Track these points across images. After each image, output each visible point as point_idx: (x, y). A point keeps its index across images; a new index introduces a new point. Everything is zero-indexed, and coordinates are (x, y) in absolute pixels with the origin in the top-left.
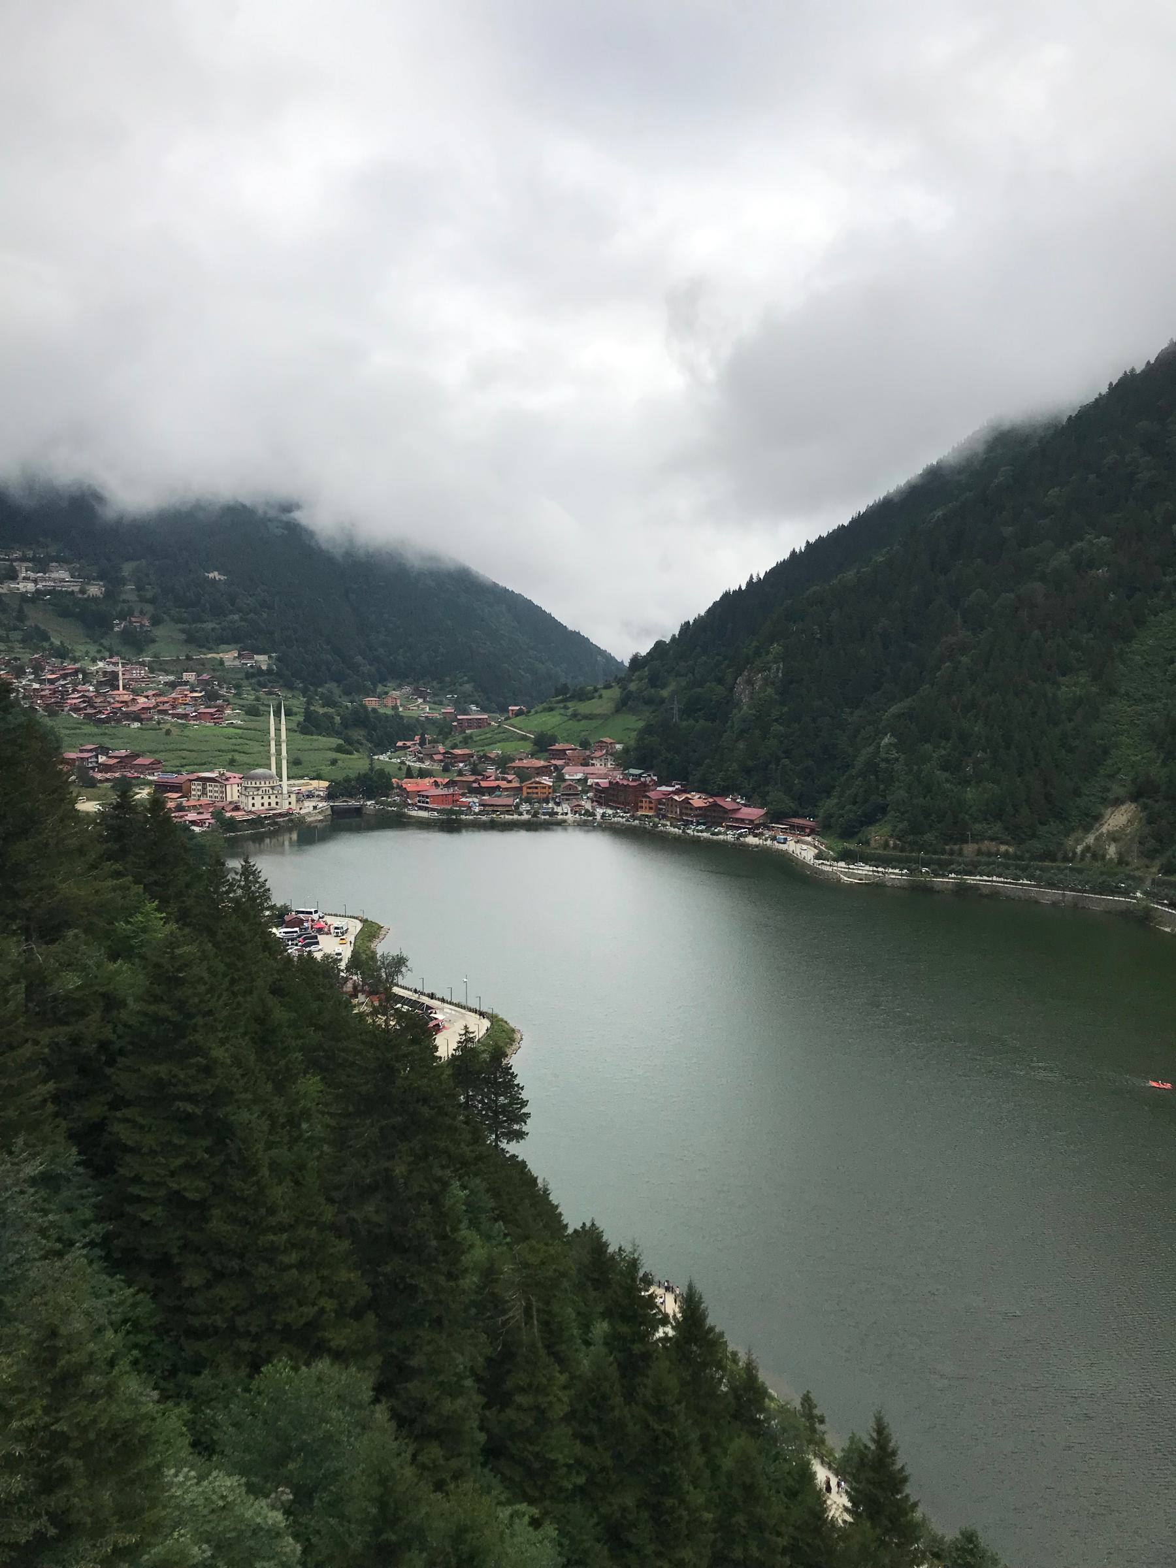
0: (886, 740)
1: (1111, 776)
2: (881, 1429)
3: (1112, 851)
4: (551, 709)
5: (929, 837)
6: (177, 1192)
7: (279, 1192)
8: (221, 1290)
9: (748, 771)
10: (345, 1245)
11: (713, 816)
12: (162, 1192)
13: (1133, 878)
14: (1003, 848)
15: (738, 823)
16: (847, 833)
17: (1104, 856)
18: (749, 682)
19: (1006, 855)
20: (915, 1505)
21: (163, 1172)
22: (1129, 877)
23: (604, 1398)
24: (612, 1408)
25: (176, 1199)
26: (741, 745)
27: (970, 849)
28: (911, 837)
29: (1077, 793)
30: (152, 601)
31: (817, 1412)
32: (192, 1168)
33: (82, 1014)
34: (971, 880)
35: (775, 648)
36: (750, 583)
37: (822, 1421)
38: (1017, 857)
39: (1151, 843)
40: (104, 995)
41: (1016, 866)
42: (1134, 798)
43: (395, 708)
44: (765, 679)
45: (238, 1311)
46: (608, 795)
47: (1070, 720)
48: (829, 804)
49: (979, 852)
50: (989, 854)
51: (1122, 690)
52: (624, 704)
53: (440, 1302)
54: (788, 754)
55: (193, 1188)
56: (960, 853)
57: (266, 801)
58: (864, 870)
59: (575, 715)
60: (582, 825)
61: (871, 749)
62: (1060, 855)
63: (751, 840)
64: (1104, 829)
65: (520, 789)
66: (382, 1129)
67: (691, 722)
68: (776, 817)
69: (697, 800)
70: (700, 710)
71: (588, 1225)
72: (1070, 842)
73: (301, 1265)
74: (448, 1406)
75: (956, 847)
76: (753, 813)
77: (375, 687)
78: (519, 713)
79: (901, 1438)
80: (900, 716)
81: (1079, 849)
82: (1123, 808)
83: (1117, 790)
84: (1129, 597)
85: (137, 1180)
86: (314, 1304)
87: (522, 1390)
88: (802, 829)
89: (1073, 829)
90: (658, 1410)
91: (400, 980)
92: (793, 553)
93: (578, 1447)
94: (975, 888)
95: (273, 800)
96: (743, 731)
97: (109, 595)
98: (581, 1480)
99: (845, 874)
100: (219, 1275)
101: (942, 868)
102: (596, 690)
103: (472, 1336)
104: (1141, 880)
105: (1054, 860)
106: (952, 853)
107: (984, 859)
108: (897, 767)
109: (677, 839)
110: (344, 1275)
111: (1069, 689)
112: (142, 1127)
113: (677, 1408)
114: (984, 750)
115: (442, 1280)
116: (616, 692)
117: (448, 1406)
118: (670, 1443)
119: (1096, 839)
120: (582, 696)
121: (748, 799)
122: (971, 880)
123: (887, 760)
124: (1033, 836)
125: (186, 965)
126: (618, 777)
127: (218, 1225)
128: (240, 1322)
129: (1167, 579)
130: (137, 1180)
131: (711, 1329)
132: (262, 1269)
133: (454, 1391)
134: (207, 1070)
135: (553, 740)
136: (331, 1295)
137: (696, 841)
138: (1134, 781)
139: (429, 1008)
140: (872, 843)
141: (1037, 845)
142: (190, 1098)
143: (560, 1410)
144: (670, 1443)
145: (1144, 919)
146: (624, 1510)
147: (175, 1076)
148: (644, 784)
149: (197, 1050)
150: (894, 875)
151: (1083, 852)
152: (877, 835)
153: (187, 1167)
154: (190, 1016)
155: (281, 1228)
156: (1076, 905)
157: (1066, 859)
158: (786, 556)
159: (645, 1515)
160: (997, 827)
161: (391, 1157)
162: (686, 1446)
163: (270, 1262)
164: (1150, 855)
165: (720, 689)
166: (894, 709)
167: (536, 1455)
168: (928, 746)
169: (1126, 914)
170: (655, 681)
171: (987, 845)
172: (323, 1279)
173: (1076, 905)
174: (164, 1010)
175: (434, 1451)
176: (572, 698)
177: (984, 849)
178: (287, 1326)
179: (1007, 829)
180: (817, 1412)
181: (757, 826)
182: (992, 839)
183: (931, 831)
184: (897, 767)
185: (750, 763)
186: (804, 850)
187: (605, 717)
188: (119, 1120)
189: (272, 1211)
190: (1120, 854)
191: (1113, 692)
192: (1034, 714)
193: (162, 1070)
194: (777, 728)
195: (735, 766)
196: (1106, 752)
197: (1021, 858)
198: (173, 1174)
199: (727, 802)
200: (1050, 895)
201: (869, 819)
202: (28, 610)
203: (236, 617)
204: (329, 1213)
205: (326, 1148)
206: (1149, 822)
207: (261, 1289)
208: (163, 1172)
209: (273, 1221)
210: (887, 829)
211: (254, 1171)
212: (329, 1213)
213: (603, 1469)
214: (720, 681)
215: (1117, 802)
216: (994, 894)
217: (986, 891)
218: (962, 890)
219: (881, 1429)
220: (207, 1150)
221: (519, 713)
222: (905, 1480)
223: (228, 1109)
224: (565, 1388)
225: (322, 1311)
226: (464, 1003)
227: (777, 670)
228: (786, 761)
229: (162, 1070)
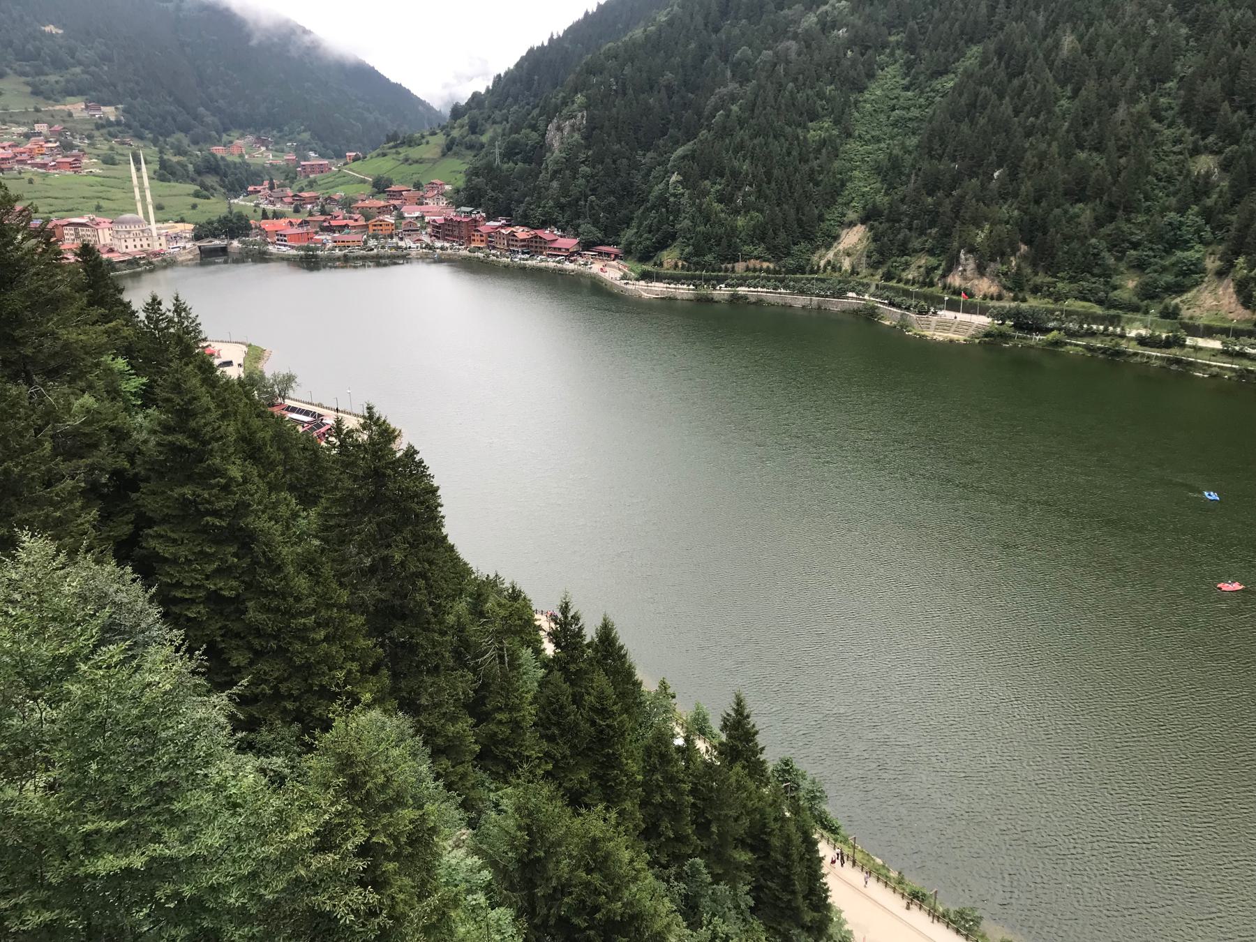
0: (674, 178)
1: (847, 204)
2: (739, 703)
3: (846, 264)
4: (384, 155)
5: (709, 258)
6: (215, 591)
7: (302, 583)
8: (263, 666)
9: (562, 208)
10: (361, 619)
11: (534, 247)
12: (202, 594)
13: (863, 285)
14: (765, 265)
15: (556, 252)
16: (645, 257)
17: (840, 268)
18: (559, 129)
19: (768, 270)
20: (763, 749)
21: (199, 577)
22: (860, 284)
23: (562, 707)
24: (568, 714)
25: (215, 598)
26: (555, 184)
27: (740, 266)
28: (695, 259)
29: (821, 218)
31: (670, 691)
32: (223, 572)
33: (95, 446)
34: (742, 290)
35: (580, 98)
36: (551, 40)
37: (674, 697)
38: (776, 272)
39: (875, 257)
40: (112, 430)
41: (777, 279)
42: (863, 223)
43: (241, 156)
44: (572, 126)
45: (280, 680)
46: (444, 230)
47: (817, 158)
48: (629, 234)
49: (748, 269)
50: (755, 270)
51: (857, 133)
52: (449, 148)
53: (436, 654)
54: (594, 190)
55: (228, 587)
56: (733, 270)
57: (138, 243)
58: (659, 288)
59: (406, 160)
60: (422, 258)
61: (661, 186)
62: (808, 268)
63: (569, 266)
64: (841, 247)
65: (367, 226)
66: (378, 525)
67: (511, 164)
68: (587, 245)
69: (521, 233)
70: (518, 154)
71: (492, 576)
72: (815, 258)
73: (326, 639)
74: (451, 729)
75: (730, 266)
76: (570, 243)
77: (220, 137)
78: (356, 159)
79: (750, 706)
80: (684, 157)
81: (822, 263)
82: (855, 229)
83: (852, 215)
84: (863, 55)
85: (178, 585)
86: (342, 668)
87: (499, 709)
88: (608, 254)
89: (818, 248)
90: (603, 711)
91: (291, 393)
92: (587, 13)
93: (545, 745)
94: (745, 297)
95: (145, 242)
96: (555, 172)
98: (550, 767)
99: (645, 291)
100: (258, 654)
101: (720, 280)
102: (423, 137)
103: (462, 676)
104: (868, 285)
105: (803, 273)
106: (726, 270)
107: (751, 274)
108: (683, 201)
109: (506, 267)
110: (363, 643)
111: (815, 132)
112: (174, 541)
113: (615, 708)
115: (436, 637)
116: (440, 139)
117: (451, 729)
118: (611, 733)
119: (835, 255)
120: (410, 142)
121: (563, 231)
122: (742, 290)
123: (675, 195)
124: (788, 254)
125: (195, 399)
126: (452, 214)
127: (253, 614)
128: (283, 688)
129: (893, 39)
130: (178, 585)
131: (622, 647)
132: (298, 646)
133: (454, 719)
134: (226, 488)
135: (390, 182)
136: (353, 659)
137: (523, 269)
138: (864, 208)
139: (320, 415)
140: (665, 265)
141: (790, 262)
142: (216, 513)
143: (530, 721)
144: (611, 733)
145: (869, 316)
146: (581, 782)
147: (199, 496)
148: (475, 221)
149: (217, 472)
150: (684, 291)
151: (825, 268)
152: (669, 258)
153: (219, 571)
154: (204, 443)
155: (306, 614)
156: (819, 307)
157: (812, 272)
158: (581, 16)
159: (595, 784)
160: (761, 248)
161: (389, 546)
162: (623, 734)
163: (304, 640)
164: (875, 266)
165: (534, 135)
166: (680, 151)
167: (514, 754)
169: (856, 312)
170: (474, 128)
171: (753, 263)
172: (345, 647)
173: (819, 307)
174: (182, 439)
175: (445, 763)
176: (403, 143)
177: (751, 266)
178: (321, 686)
179: (768, 249)
180: (670, 691)
181: (572, 254)
182: (757, 258)
183: (712, 253)
184: (683, 201)
185: (562, 200)
186: (611, 272)
187: (434, 161)
188: (152, 537)
189: (298, 599)
190: (853, 268)
191: (849, 135)
192: (789, 154)
193: (187, 491)
194: (584, 169)
195: (551, 203)
196: (843, 185)
197: (779, 272)
198: (207, 578)
199: (546, 234)
200: (800, 301)
201: (662, 245)
203: (78, 70)
204: (345, 596)
205: (317, 542)
206: (875, 240)
207: (298, 661)
208: (199, 577)
209: (301, 607)
210: (676, 253)
211: (279, 568)
212: (345, 596)
213: (564, 757)
214: (534, 128)
215: (851, 224)
216: (759, 302)
217: (753, 300)
218: (735, 298)
219: (739, 703)
220: (235, 555)
221: (356, 159)
222: (757, 733)
223: (250, 519)
224: (531, 704)
225: (350, 672)
226: (349, 410)
227: (581, 118)
228: (593, 198)
229: (187, 491)
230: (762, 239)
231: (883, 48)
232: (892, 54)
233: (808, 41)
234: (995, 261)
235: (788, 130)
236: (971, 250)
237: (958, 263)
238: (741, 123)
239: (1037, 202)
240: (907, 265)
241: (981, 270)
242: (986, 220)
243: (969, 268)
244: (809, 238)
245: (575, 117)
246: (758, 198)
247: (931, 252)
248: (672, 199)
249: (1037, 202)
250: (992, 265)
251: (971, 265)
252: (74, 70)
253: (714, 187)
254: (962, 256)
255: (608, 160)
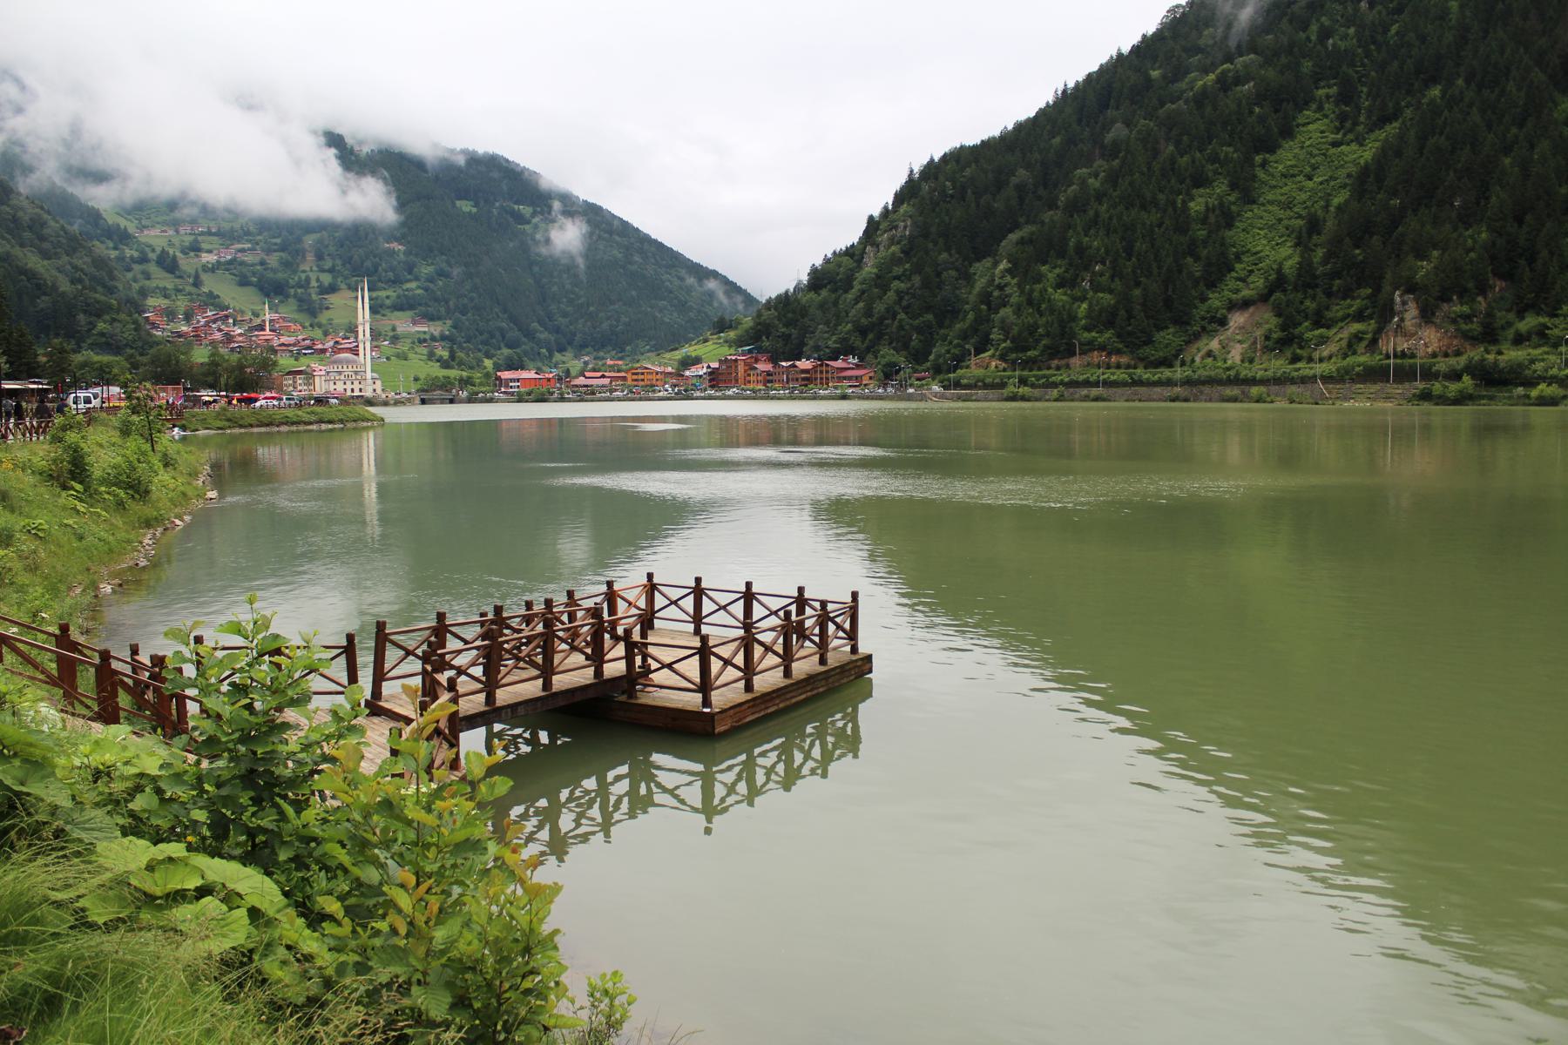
4: (706, 341)
30: (330, 271)
57: (349, 386)
75: (1063, 362)
77: (551, 356)
95: (356, 386)
96: (863, 292)
97: (287, 265)
114: (1103, 263)
129: (1321, 92)
168: (1044, 268)
179: (1119, 336)
182: (1102, 348)
185: (864, 321)
194: (896, 284)
202: (204, 277)
203: (413, 285)
230: (1110, 324)
231: (1306, 103)
232: (1320, 108)
233: (1202, 99)
234: (1449, 300)
235: (1161, 197)
236: (1411, 288)
237: (1393, 314)
238: (1100, 196)
239: (1519, 221)
240: (1323, 340)
241: (1427, 315)
242: (1435, 247)
243: (1408, 316)
244: (1182, 321)
245: (896, 227)
246: (1112, 278)
247: (1359, 317)
248: (996, 293)
249: (1519, 221)
250: (1445, 306)
251: (1412, 312)
252: (408, 285)
253: (1050, 273)
254: (1398, 299)
255: (928, 269)
